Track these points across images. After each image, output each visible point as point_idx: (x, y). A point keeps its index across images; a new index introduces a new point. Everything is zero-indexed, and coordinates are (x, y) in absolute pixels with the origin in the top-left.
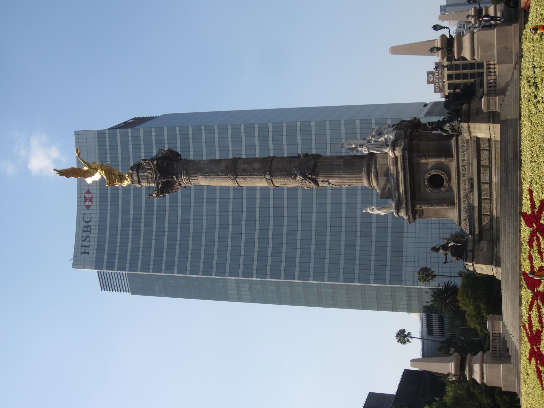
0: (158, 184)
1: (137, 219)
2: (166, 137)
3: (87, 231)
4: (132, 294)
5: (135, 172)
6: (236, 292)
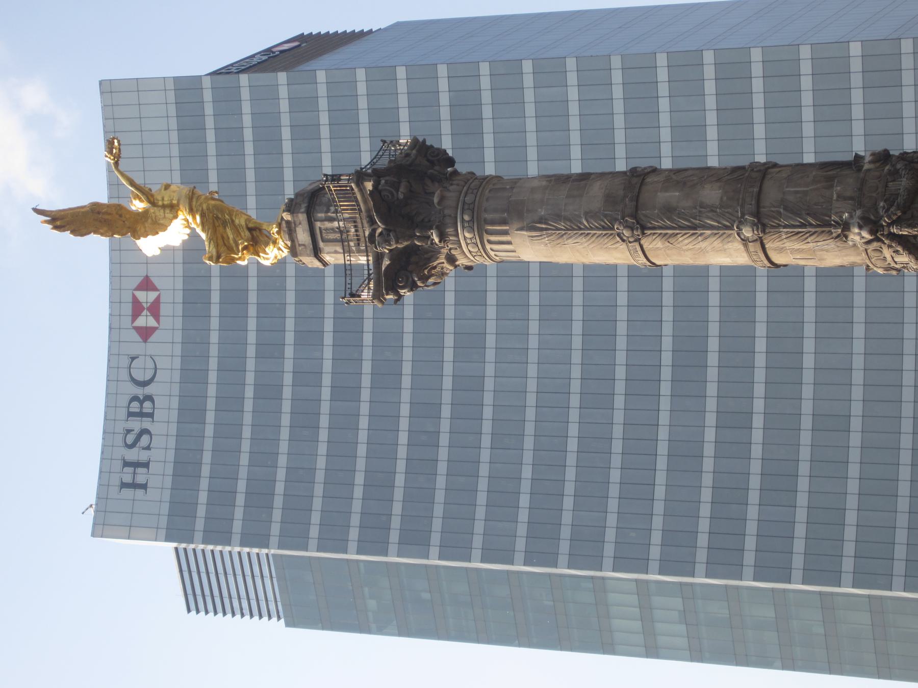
0: (379, 258)
1: (307, 376)
2: (403, 101)
3: (141, 414)
4: (288, 625)
5: (302, 217)
6: (637, 625)
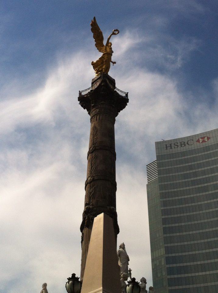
3: (181, 145)
4: (147, 185)
